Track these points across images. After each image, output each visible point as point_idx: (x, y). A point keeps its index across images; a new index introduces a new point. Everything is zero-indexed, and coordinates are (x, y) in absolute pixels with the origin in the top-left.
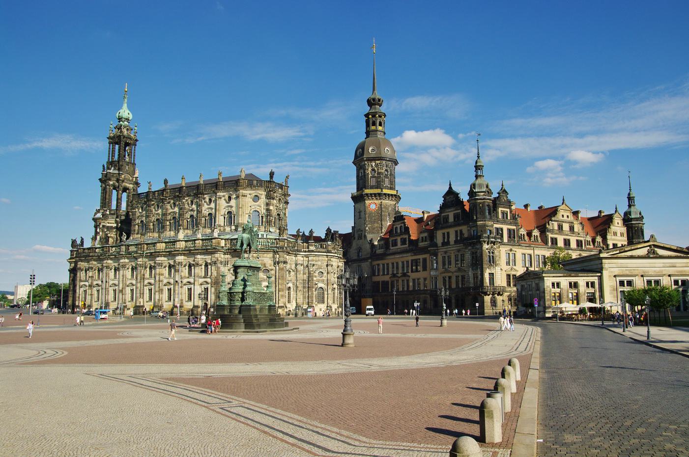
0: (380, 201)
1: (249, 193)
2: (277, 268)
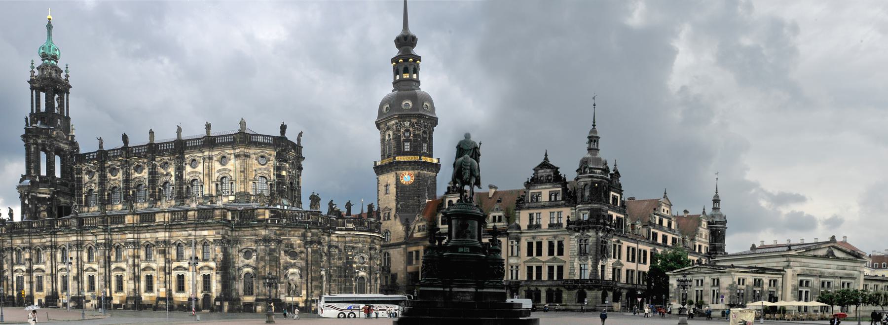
1: (252, 151)
2: (309, 250)
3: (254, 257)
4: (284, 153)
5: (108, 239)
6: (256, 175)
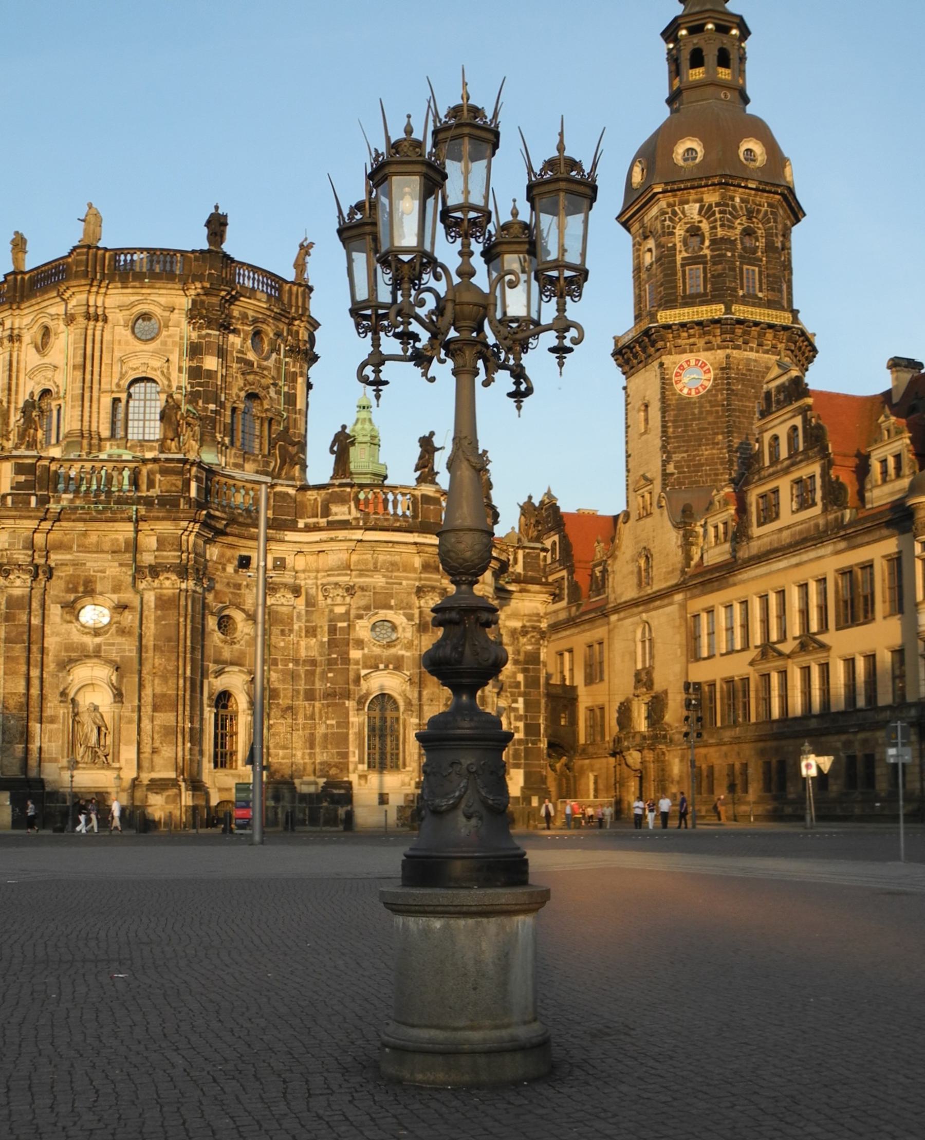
0: (721, 354)
4: (215, 300)
6: (122, 376)
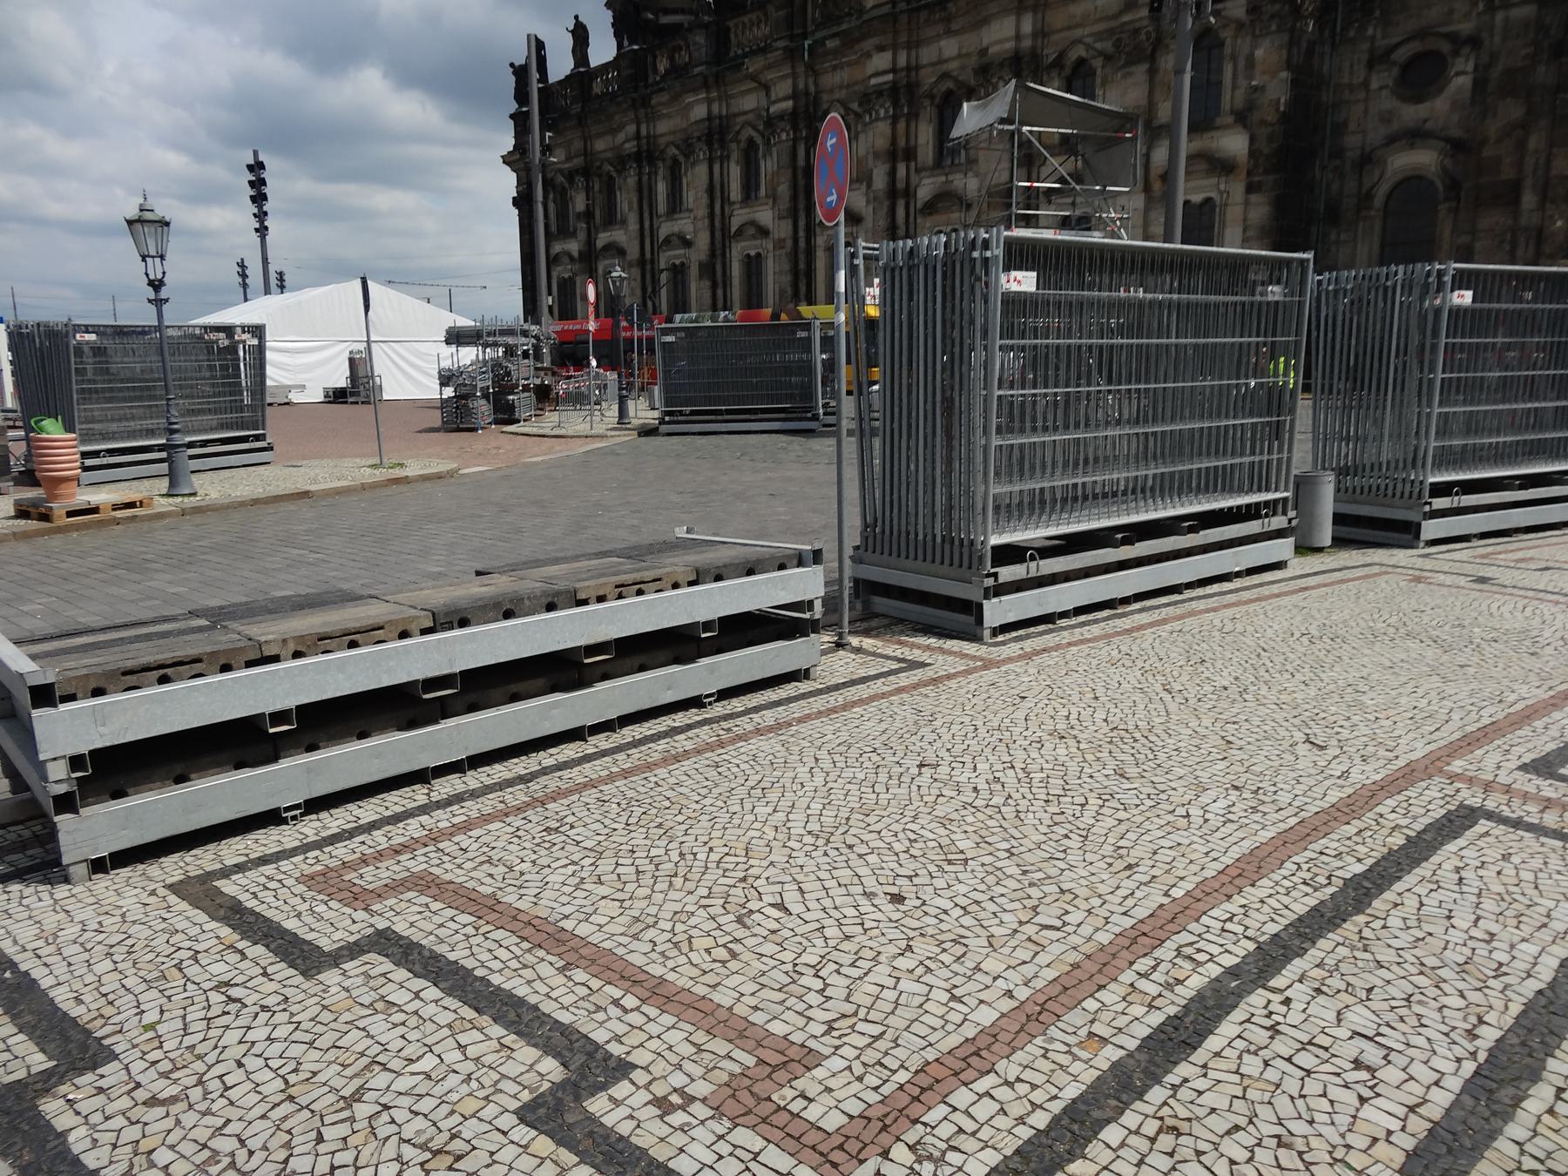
3: (1460, 82)
5: (807, 93)
